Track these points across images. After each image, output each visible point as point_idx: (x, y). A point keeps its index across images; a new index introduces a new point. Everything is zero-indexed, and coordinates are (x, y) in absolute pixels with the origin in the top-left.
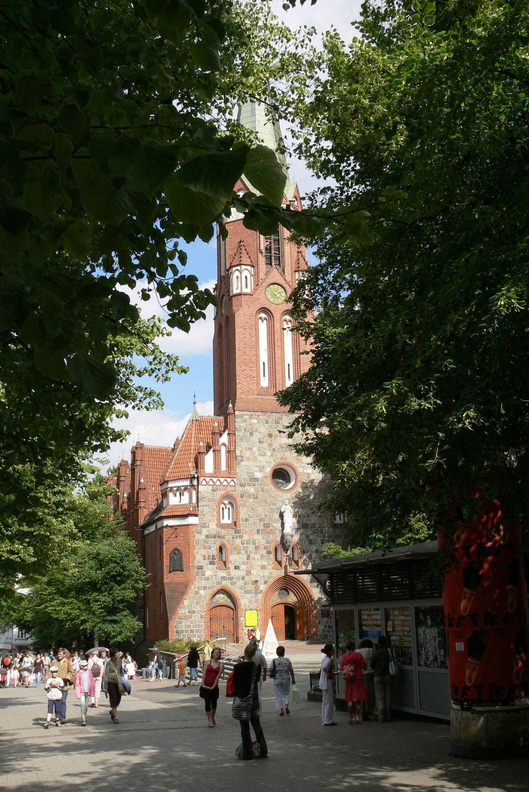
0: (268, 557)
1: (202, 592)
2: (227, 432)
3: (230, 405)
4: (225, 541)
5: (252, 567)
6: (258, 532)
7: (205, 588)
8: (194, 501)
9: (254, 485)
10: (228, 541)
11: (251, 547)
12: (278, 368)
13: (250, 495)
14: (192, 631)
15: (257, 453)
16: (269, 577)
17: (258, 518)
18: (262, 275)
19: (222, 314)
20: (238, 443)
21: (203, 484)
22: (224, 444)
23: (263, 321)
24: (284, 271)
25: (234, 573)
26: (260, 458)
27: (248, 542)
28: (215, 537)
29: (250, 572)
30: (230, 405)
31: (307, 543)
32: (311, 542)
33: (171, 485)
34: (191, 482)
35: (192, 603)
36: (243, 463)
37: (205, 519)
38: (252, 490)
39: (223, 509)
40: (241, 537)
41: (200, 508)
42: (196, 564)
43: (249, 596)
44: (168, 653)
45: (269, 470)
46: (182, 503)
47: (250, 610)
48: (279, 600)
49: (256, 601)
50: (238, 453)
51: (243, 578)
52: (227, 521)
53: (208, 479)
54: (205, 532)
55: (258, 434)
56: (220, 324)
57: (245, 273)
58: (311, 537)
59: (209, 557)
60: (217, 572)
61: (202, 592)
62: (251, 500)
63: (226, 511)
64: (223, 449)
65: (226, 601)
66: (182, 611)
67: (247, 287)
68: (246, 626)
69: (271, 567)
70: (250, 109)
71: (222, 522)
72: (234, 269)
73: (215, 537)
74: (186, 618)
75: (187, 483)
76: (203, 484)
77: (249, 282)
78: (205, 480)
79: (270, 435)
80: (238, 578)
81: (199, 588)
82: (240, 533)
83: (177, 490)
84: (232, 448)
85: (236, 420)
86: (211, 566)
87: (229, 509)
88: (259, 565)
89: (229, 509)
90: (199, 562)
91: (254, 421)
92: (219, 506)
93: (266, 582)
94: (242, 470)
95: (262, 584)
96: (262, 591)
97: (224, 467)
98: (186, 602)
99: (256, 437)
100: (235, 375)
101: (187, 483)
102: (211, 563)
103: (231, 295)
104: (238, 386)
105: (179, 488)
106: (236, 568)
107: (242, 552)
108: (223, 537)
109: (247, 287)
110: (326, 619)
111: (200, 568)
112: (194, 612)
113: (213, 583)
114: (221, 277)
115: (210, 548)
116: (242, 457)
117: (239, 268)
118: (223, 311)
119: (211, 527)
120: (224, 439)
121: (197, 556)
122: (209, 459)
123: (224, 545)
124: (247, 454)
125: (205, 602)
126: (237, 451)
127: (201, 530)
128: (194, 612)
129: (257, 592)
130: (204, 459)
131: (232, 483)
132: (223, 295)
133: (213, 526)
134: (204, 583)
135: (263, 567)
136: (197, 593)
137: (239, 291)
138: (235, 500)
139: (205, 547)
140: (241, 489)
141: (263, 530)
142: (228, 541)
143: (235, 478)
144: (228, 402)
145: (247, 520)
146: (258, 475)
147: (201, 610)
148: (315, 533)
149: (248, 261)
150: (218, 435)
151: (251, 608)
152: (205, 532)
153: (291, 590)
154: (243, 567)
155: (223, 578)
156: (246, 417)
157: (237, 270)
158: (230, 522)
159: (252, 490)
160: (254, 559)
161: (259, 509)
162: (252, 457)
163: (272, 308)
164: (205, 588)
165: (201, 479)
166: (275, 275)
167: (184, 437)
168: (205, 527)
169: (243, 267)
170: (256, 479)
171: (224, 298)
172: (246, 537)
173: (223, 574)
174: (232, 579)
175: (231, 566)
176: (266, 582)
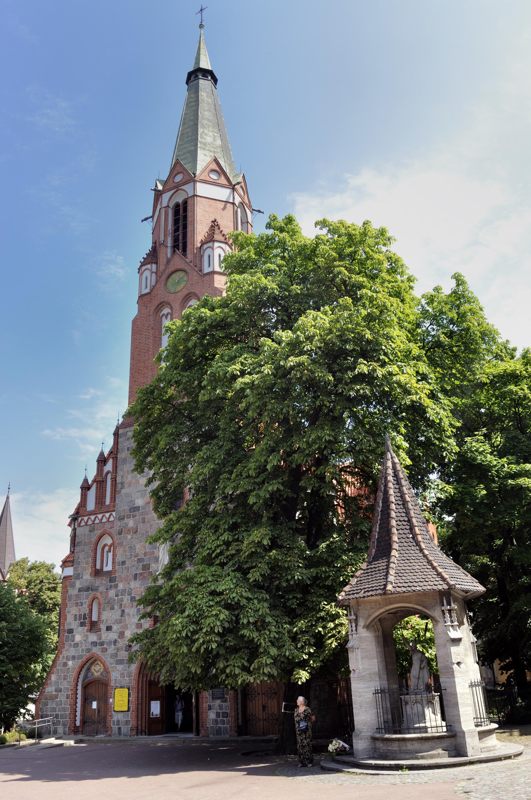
4: (98, 595)
5: (126, 627)
6: (135, 577)
7: (74, 658)
9: (134, 516)
10: (101, 593)
11: (126, 599)
13: (129, 530)
14: (57, 716)
17: (136, 559)
20: (119, 467)
22: (108, 472)
27: (123, 592)
28: (88, 589)
29: (124, 632)
35: (59, 677)
36: (123, 491)
37: (80, 569)
38: (131, 523)
40: (116, 586)
41: (76, 556)
42: (66, 627)
43: (120, 667)
47: (121, 687)
49: (129, 676)
50: (119, 480)
51: (115, 642)
52: (108, 568)
53: (86, 518)
54: (78, 585)
59: (80, 615)
60: (87, 636)
61: (70, 663)
62: (129, 537)
68: (114, 711)
71: (105, 569)
73: (88, 589)
80: (110, 643)
81: (68, 658)
82: (115, 581)
86: (80, 629)
90: (70, 624)
97: (108, 502)
102: (82, 624)
106: (109, 628)
107: (116, 606)
108: (96, 590)
110: (218, 702)
111: (71, 631)
112: (60, 691)
113: (83, 650)
115: (82, 605)
116: (122, 483)
119: (84, 577)
125: (72, 676)
127: (74, 583)
128: (60, 691)
131: (112, 519)
133: (87, 576)
134: (72, 652)
136: (65, 664)
139: (77, 604)
140: (119, 523)
141: (141, 574)
142: (101, 593)
143: (114, 511)
145: (123, 563)
147: (68, 688)
151: (123, 684)
152: (78, 585)
154: (115, 627)
155: (94, 644)
159: (131, 523)
160: (129, 615)
161: (138, 546)
162: (134, 481)
164: (74, 658)
168: (79, 579)
170: (138, 508)
172: (121, 586)
173: (93, 637)
174: (102, 644)
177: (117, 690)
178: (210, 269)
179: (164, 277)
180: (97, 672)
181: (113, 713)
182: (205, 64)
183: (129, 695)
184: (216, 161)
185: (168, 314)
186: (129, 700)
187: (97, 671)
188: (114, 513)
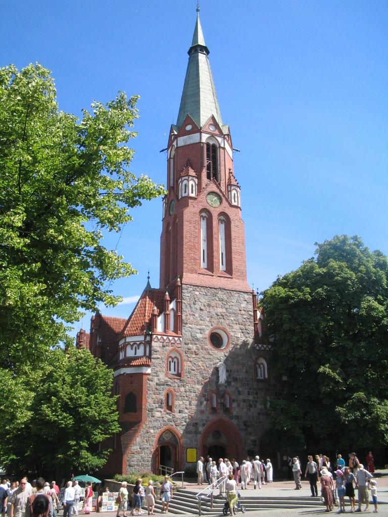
1: (152, 431)
2: (175, 300)
3: (179, 280)
4: (172, 389)
7: (154, 428)
8: (148, 354)
12: (215, 254)
15: (199, 319)
16: (207, 421)
18: (203, 185)
19: (170, 215)
21: (155, 340)
23: (203, 220)
24: (220, 184)
25: (178, 415)
26: (201, 322)
28: (163, 385)
30: (179, 280)
31: (237, 393)
32: (239, 393)
33: (129, 339)
34: (145, 338)
38: (194, 348)
39: (170, 362)
44: (131, 485)
45: (207, 333)
46: (137, 355)
47: (191, 448)
50: (184, 317)
53: (159, 337)
54: (156, 380)
55: (200, 303)
56: (169, 223)
57: (191, 183)
58: (240, 389)
61: (152, 431)
63: (172, 364)
64: (172, 314)
65: (170, 439)
66: (134, 448)
67: (192, 192)
69: (208, 412)
70: (195, 73)
72: (183, 178)
74: (138, 453)
75: (142, 338)
76: (155, 340)
77: (194, 189)
78: (158, 338)
79: (209, 305)
83: (133, 344)
84: (179, 314)
85: (183, 291)
87: (175, 362)
89: (175, 362)
91: (197, 293)
92: (168, 360)
93: (204, 425)
94: (186, 331)
96: (201, 432)
98: (138, 439)
99: (197, 306)
100: (182, 257)
101: (142, 338)
103: (180, 197)
104: (185, 265)
105: (135, 343)
106: (180, 412)
109: (192, 192)
114: (170, 187)
117: (186, 178)
118: (171, 213)
120: (172, 306)
121: (150, 400)
122: (160, 320)
123: (171, 392)
124: (191, 318)
126: (183, 316)
129: (196, 433)
130: (156, 320)
132: (172, 200)
137: (186, 194)
138: (180, 355)
144: (175, 277)
146: (199, 336)
148: (243, 386)
149: (194, 174)
150: (169, 302)
155: (169, 420)
156: (191, 289)
157: (186, 179)
158: (176, 373)
163: (211, 209)
165: (154, 336)
166: (213, 187)
167: (139, 304)
169: (190, 178)
170: (198, 339)
171: (173, 203)
175: (176, 410)
176: (204, 425)
177: (188, 450)
178: (236, 204)
179: (206, 192)
180: (167, 438)
181: (186, 463)
182: (201, 42)
184: (213, 118)
185: (205, 217)
187: (167, 438)
188: (181, 339)
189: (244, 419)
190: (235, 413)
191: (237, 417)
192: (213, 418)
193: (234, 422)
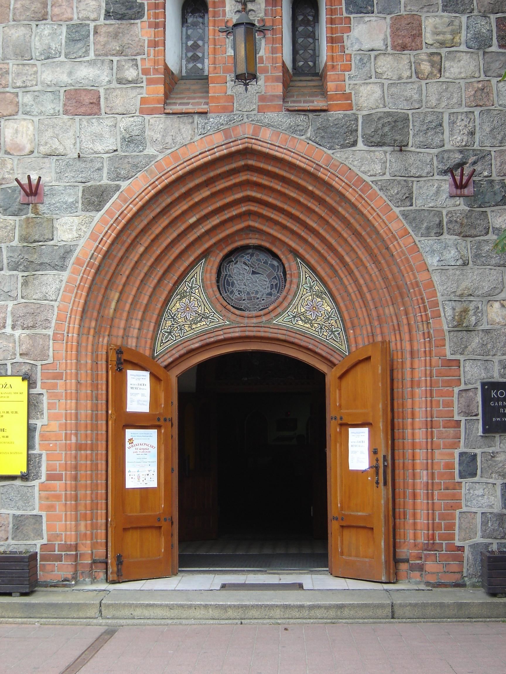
0: (116, 36)
16: (122, 165)
48: (218, 320)
49: (30, 318)
88: (52, 90)
93: (95, 198)
95: (70, 208)
96: (68, 252)
129: (33, 257)
135: (83, 103)
153: (296, 254)
176: (95, 198)
183: (33, 405)
186: (31, 430)
189: (454, 139)
190: (368, 97)
191: (390, 133)
192: (177, 142)
193: (365, 165)
